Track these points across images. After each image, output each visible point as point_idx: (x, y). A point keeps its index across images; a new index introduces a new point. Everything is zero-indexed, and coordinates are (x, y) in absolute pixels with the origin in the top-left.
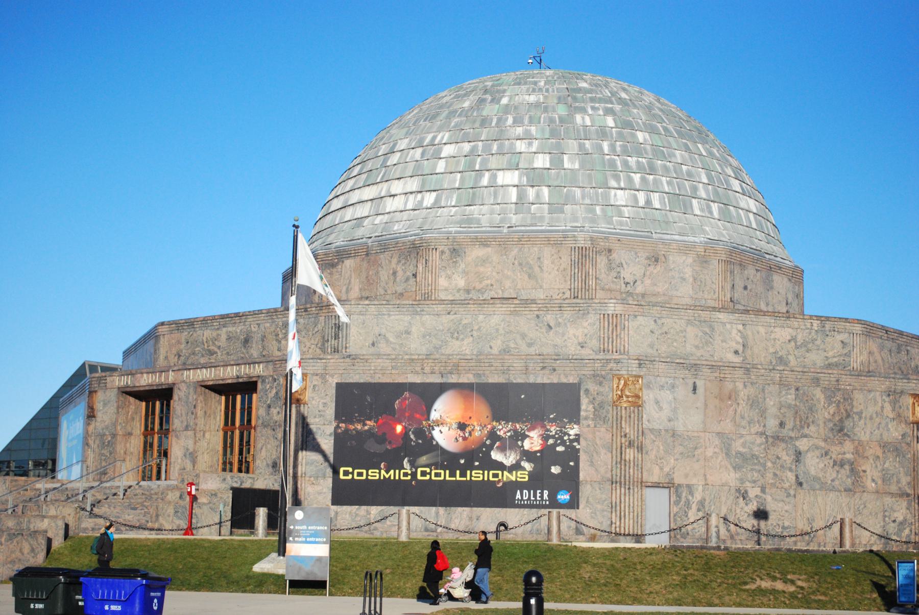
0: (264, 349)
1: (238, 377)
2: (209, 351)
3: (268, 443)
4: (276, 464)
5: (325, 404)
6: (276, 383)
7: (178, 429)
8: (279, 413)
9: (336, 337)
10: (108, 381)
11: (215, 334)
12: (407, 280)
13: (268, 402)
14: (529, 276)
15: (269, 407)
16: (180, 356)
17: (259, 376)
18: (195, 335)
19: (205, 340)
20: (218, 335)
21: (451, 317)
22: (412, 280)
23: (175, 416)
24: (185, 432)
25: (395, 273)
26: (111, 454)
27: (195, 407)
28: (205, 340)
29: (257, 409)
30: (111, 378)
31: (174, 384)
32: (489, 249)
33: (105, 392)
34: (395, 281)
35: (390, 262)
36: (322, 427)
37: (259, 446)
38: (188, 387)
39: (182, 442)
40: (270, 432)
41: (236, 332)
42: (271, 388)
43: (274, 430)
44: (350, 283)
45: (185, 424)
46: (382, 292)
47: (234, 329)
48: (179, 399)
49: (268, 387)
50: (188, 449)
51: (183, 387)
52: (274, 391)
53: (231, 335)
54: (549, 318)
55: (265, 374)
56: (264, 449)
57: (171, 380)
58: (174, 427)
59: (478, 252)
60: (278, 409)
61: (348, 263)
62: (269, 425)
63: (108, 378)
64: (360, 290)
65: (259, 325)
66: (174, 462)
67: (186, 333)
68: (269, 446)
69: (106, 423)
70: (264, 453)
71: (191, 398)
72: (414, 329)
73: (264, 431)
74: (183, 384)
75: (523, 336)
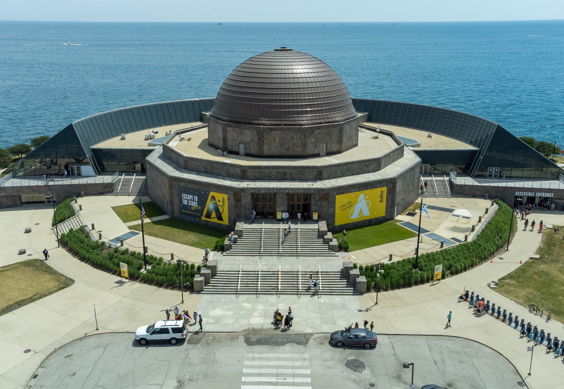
0: (292, 177)
2: (269, 176)
9: (320, 175)
12: (298, 139)
14: (330, 137)
15: (317, 201)
16: (255, 176)
21: (347, 166)
22: (300, 140)
25: (293, 137)
31: (276, 193)
32: (320, 130)
34: (293, 139)
35: (291, 134)
42: (317, 197)
44: (275, 138)
45: (282, 204)
46: (288, 142)
51: (281, 194)
54: (367, 164)
58: (278, 205)
59: (318, 131)
61: (274, 132)
64: (279, 141)
71: (284, 197)
72: (338, 171)
75: (362, 169)
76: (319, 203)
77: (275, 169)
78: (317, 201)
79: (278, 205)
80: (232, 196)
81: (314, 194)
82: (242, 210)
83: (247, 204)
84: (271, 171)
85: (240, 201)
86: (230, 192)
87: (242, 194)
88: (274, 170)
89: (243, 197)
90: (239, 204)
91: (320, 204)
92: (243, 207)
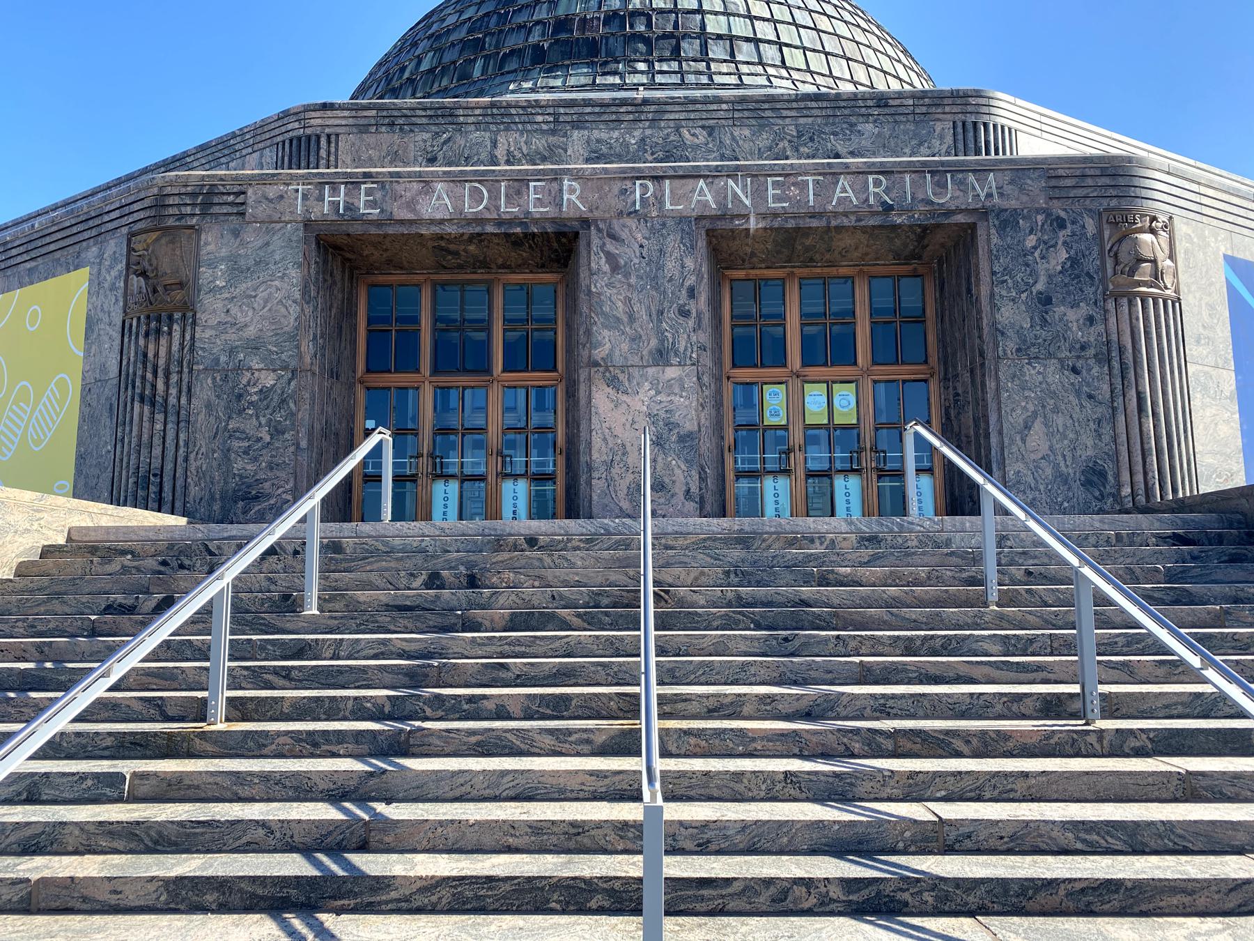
1: (888, 208)
3: (1056, 410)
4: (1102, 475)
5: (1211, 307)
6: (1062, 233)
7: (618, 361)
8: (1091, 320)
10: (250, 201)
11: (539, 143)
13: (1040, 286)
15: (1046, 300)
17: (984, 213)
18: (460, 141)
19: (502, 158)
20: (550, 148)
23: (599, 320)
24: (651, 371)
26: (277, 431)
27: (692, 293)
28: (502, 158)
29: (994, 307)
30: (272, 192)
31: (586, 222)
33: (236, 233)
36: (1214, 372)
37: (1015, 418)
38: (652, 230)
39: (642, 400)
40: (1055, 376)
41: (627, 145)
42: (1050, 246)
43: (1075, 370)
45: (654, 343)
47: (616, 134)
48: (615, 268)
49: (1031, 241)
50: (670, 425)
51: (634, 233)
52: (1064, 255)
53: (604, 149)
55: (1013, 204)
56: (1038, 426)
57: (573, 199)
58: (599, 354)
60: (1084, 309)
62: (1050, 355)
63: (250, 192)
65: (710, 130)
66: (610, 465)
67: (429, 135)
68: (1060, 421)
69: (251, 332)
70: (1037, 439)
71: (671, 266)
73: (1032, 373)
74: (631, 222)
76: (1072, 315)
77: (578, 124)
78: (1046, 300)
79: (599, 354)
80: (113, 288)
81: (1008, 221)
82: (201, 419)
83: (254, 346)
84: (539, 143)
85: (188, 312)
86: (101, 256)
87: (214, 242)
88: (576, 134)
89: (213, 276)
90: (162, 350)
91: (1092, 335)
92: (204, 390)
